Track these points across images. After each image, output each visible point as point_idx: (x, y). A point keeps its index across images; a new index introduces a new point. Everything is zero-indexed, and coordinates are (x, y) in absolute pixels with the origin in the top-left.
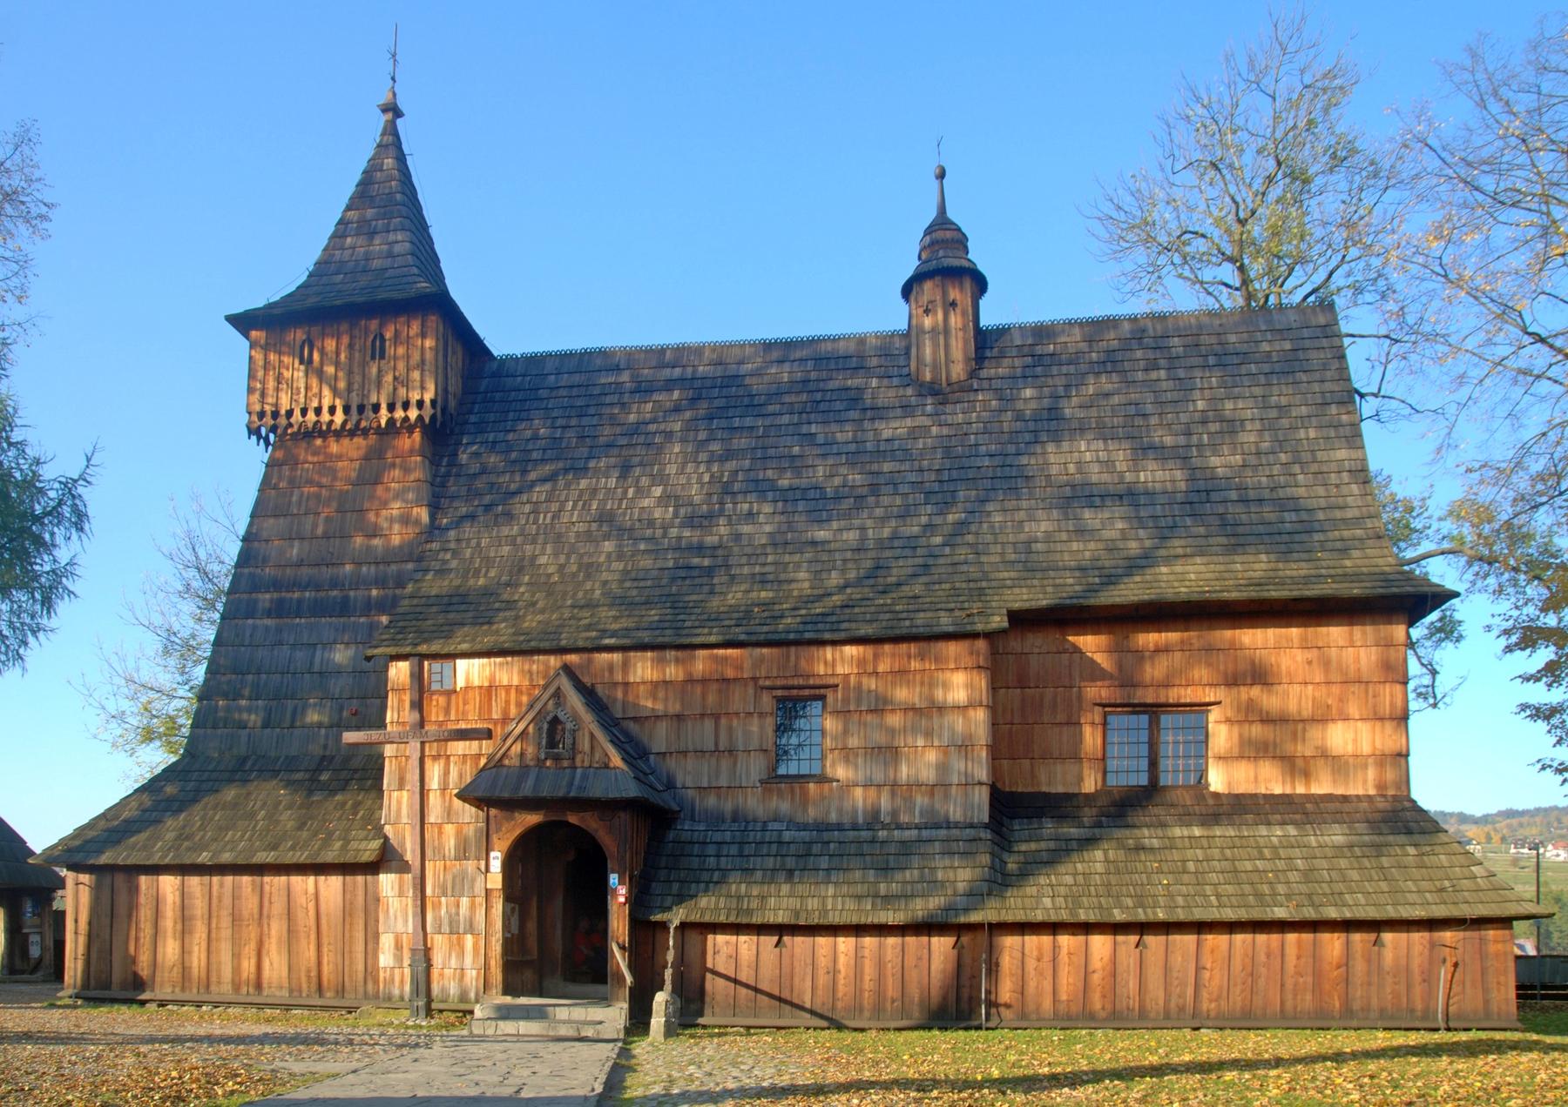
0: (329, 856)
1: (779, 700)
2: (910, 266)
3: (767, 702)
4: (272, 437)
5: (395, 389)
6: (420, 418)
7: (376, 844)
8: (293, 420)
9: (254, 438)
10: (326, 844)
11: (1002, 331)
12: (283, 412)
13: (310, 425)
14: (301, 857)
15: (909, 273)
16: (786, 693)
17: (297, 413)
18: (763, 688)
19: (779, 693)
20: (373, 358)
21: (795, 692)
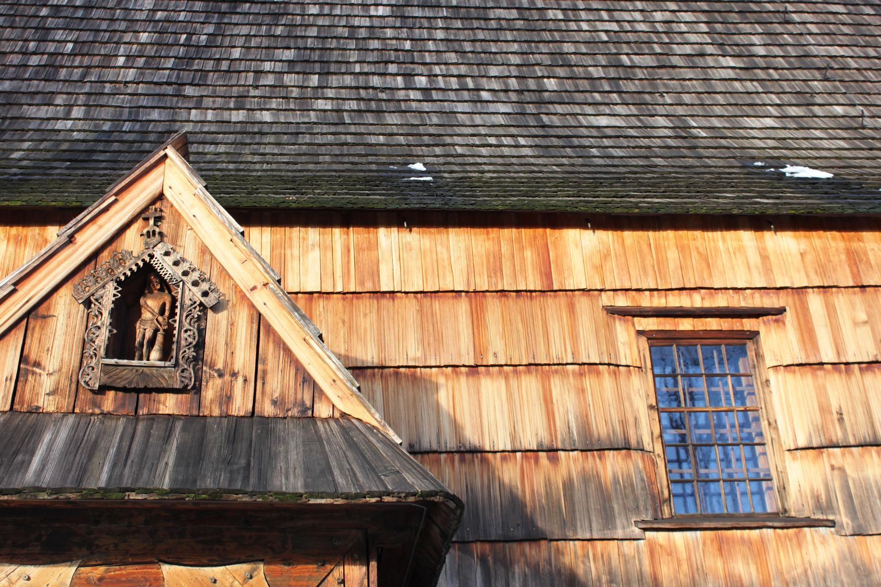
1: (658, 341)
3: (627, 343)
16: (667, 324)
18: (613, 312)
19: (651, 324)
21: (686, 325)
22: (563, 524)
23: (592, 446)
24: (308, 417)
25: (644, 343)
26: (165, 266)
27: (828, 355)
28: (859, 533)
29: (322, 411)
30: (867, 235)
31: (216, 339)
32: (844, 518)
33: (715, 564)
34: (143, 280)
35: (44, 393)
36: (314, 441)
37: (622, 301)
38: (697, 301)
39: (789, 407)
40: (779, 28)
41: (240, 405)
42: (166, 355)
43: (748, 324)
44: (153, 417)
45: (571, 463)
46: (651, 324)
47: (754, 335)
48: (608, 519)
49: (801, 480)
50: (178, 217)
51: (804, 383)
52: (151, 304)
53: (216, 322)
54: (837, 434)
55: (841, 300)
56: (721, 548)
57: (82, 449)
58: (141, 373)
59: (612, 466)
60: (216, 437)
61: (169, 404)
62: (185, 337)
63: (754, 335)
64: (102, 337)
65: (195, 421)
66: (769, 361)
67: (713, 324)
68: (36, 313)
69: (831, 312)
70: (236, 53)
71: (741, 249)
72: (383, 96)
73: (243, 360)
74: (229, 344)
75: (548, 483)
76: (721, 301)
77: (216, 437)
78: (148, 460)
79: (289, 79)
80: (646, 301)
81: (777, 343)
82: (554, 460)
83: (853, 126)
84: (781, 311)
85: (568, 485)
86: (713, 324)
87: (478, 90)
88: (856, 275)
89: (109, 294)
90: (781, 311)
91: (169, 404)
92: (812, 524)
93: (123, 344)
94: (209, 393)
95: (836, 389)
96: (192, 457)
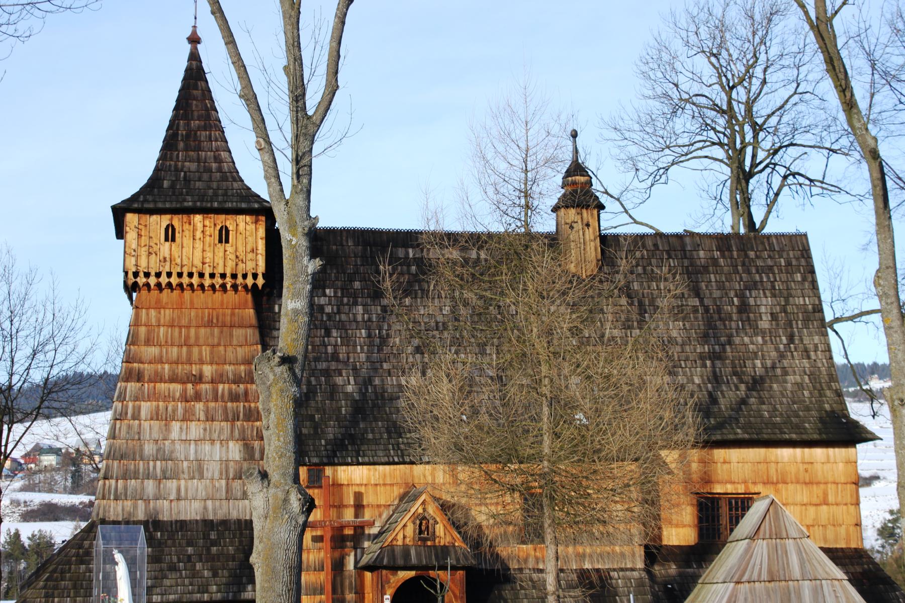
5: (237, 265)
6: (255, 285)
24: (454, 546)
31: (437, 530)
34: (424, 518)
36: (456, 552)
41: (442, 544)
53: (437, 526)
57: (418, 555)
60: (439, 551)
61: (429, 543)
65: (435, 546)
68: (405, 526)
73: (442, 534)
77: (439, 551)
89: (418, 522)
91: (429, 543)
93: (421, 532)
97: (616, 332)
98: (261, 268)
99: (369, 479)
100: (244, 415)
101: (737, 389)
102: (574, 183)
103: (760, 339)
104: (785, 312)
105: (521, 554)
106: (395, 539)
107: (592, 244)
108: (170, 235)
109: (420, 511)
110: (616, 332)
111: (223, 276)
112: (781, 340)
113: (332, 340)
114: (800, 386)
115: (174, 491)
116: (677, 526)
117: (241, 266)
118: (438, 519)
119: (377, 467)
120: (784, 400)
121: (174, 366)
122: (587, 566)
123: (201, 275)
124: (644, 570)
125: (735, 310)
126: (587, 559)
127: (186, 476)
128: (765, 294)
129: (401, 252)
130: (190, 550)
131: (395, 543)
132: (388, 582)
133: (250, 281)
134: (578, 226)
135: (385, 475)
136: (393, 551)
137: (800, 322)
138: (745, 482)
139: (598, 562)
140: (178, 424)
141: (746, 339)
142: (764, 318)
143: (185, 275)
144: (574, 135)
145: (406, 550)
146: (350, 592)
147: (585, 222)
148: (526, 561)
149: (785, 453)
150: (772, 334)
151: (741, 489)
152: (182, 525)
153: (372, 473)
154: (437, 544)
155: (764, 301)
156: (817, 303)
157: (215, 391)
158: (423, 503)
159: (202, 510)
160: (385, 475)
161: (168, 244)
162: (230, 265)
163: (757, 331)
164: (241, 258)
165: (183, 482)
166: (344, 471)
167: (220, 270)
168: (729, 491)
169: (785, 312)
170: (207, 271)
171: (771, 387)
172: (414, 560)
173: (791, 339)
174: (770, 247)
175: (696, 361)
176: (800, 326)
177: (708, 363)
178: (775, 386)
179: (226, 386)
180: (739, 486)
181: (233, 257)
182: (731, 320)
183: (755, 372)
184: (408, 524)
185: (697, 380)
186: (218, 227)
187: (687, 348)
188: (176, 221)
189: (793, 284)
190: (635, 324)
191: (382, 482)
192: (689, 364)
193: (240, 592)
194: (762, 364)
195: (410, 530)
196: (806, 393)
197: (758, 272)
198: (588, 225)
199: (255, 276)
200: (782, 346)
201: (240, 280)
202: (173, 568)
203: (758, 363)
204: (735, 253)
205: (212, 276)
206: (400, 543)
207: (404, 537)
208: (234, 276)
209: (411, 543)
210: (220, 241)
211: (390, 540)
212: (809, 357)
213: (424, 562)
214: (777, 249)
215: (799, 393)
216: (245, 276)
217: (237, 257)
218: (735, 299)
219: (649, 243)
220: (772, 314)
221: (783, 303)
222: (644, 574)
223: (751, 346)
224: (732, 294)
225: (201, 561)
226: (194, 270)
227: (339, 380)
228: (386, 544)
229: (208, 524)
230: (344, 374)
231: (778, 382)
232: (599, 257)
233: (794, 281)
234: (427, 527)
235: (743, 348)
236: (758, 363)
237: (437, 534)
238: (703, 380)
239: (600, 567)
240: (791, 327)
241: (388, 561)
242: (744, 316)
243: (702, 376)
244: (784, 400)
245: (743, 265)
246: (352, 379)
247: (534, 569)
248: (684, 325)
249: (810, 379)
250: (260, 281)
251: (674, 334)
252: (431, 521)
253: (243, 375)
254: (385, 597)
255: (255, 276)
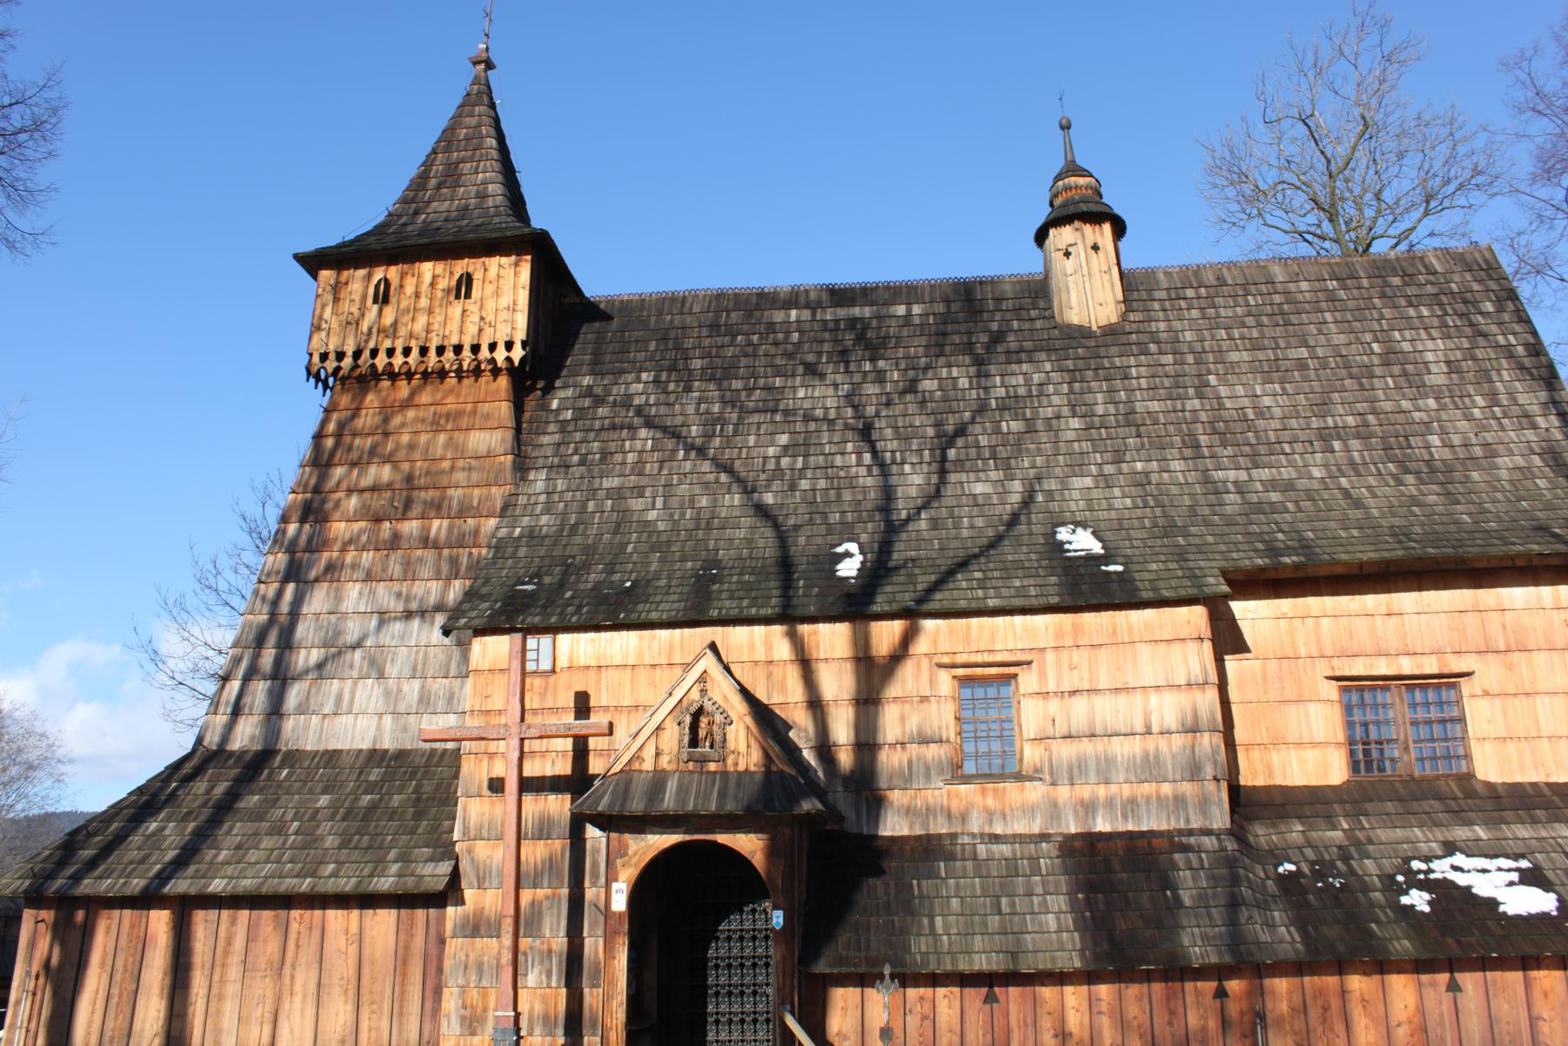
0: (385, 884)
2: (1042, 213)
4: (331, 380)
5: (481, 330)
7: (445, 868)
8: (360, 362)
9: (312, 380)
10: (379, 866)
11: (1150, 274)
12: (350, 353)
13: (380, 368)
14: (347, 884)
15: (1040, 220)
17: (366, 354)
18: (940, 666)
19: (960, 672)
20: (458, 297)
21: (979, 671)
22: (906, 781)
23: (924, 741)
25: (956, 682)
26: (708, 706)
27: (1052, 687)
28: (1053, 784)
29: (774, 769)
30: (1086, 615)
31: (730, 737)
32: (1047, 777)
33: (979, 799)
35: (665, 762)
37: (946, 660)
38: (988, 658)
39: (1031, 716)
40: (1118, 384)
41: (741, 768)
42: (712, 747)
43: (1012, 670)
44: (708, 772)
45: (914, 749)
46: (960, 672)
47: (1015, 676)
48: (928, 778)
49: (1031, 755)
50: (713, 680)
51: (1040, 702)
52: (704, 721)
53: (731, 730)
54: (1051, 733)
55: (1064, 654)
56: (984, 792)
57: (682, 790)
58: (703, 755)
59: (932, 751)
60: (732, 782)
62: (718, 738)
63: (1015, 676)
64: (686, 739)
65: (725, 774)
66: (1022, 691)
67: (994, 671)
68: (659, 728)
69: (1058, 663)
70: (752, 440)
71: (1013, 626)
72: (842, 474)
73: (742, 747)
74: (736, 739)
75: (900, 761)
76: (999, 658)
77: (732, 782)
78: (707, 797)
79: (785, 461)
80: (960, 659)
81: (1027, 681)
82: (904, 749)
83: (1141, 481)
84: (1029, 663)
85: (910, 762)
86: (994, 671)
87: (903, 463)
88: (1075, 639)
89: (688, 719)
90: (1029, 663)
91: (712, 767)
92: (1031, 779)
93: (694, 742)
94: (730, 761)
95: (1054, 706)
96: (723, 795)
97: (1155, 406)
98: (520, 335)
99: (640, 654)
100: (469, 568)
101: (1400, 483)
102: (1067, 188)
103: (1432, 403)
104: (1475, 359)
105: (954, 805)
106: (637, 757)
107: (1106, 277)
108: (383, 297)
109: (695, 695)
110: (1155, 406)
111: (458, 349)
112: (1473, 402)
113: (638, 444)
114: (1526, 472)
115: (332, 700)
116: (1299, 744)
117: (488, 331)
118: (734, 716)
119: (657, 632)
120: (1499, 496)
121: (367, 495)
122: (1102, 825)
123: (424, 351)
124: (1230, 832)
125: (1376, 360)
126: (1100, 812)
127: (355, 674)
128: (1429, 334)
129: (778, 316)
130: (324, 800)
131: (636, 766)
132: (623, 852)
133: (500, 355)
134: (1080, 251)
135: (671, 647)
136: (628, 783)
137: (1504, 373)
138: (1438, 652)
139: (1125, 817)
140: (358, 586)
141: (1405, 404)
142: (1434, 368)
143: (399, 351)
144: (1066, 127)
145: (658, 780)
146: (594, 884)
147: (1090, 243)
148: (964, 818)
149: (1517, 596)
150: (1453, 396)
151: (1431, 666)
152: (331, 757)
153: (646, 644)
154: (731, 768)
155: (1430, 345)
156: (1531, 340)
157: (425, 532)
158: (703, 678)
159: (372, 732)
160: (671, 647)
161: (376, 307)
162: (472, 329)
163: (1422, 389)
164: (488, 319)
165: (349, 683)
166: (593, 640)
167: (454, 340)
168: (1407, 671)
169: (1475, 359)
170: (434, 343)
171: (1467, 480)
172: (669, 802)
173: (1493, 397)
174: (1425, 266)
175: (1311, 443)
176: (1507, 378)
177: (1337, 445)
178: (1475, 475)
179: (446, 523)
180: (1425, 659)
181: (477, 319)
182: (1372, 376)
183: (1431, 454)
184: (668, 724)
185: (1317, 473)
186: (457, 276)
187: (1294, 423)
188: (393, 272)
189: (1479, 318)
190: (1191, 391)
191: (664, 661)
192: (1298, 447)
193: (371, 875)
194: (1442, 441)
195: (673, 738)
196: (1541, 483)
197: (1411, 305)
198: (1095, 248)
199: (509, 346)
200: (1477, 413)
201: (485, 353)
202: (279, 830)
203: (1435, 440)
204: (1365, 282)
205: (441, 350)
206: (648, 765)
207: (658, 754)
208: (476, 349)
209: (672, 767)
210: (458, 297)
211: (625, 759)
212: (1535, 427)
213: (690, 807)
214: (1439, 269)
215: (1528, 483)
216: (493, 347)
217: (482, 318)
218: (1375, 346)
219: (1210, 278)
220: (1447, 362)
221: (1467, 345)
222: (1231, 845)
223: (1416, 415)
224: (1368, 337)
225: (332, 818)
226: (413, 343)
227: (636, 504)
228: (617, 768)
229: (375, 756)
230: (648, 494)
231: (1480, 469)
232: (1120, 297)
233: (1481, 313)
234: (710, 733)
235: (1400, 418)
236: (1435, 440)
237: (731, 745)
238: (1328, 471)
239: (1130, 828)
240: (1491, 381)
241: (612, 804)
242: (1396, 369)
243: (1326, 466)
244: (1499, 496)
245: (1383, 296)
246: (659, 502)
247: (982, 835)
248: (1283, 389)
249: (1543, 460)
250: (518, 353)
251: (1267, 401)
252: (718, 718)
253: (475, 503)
254: (615, 886)
255: (509, 346)
